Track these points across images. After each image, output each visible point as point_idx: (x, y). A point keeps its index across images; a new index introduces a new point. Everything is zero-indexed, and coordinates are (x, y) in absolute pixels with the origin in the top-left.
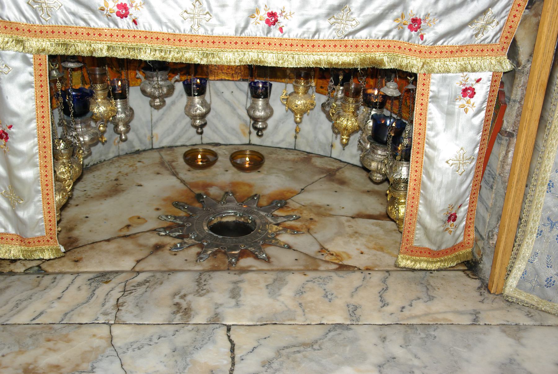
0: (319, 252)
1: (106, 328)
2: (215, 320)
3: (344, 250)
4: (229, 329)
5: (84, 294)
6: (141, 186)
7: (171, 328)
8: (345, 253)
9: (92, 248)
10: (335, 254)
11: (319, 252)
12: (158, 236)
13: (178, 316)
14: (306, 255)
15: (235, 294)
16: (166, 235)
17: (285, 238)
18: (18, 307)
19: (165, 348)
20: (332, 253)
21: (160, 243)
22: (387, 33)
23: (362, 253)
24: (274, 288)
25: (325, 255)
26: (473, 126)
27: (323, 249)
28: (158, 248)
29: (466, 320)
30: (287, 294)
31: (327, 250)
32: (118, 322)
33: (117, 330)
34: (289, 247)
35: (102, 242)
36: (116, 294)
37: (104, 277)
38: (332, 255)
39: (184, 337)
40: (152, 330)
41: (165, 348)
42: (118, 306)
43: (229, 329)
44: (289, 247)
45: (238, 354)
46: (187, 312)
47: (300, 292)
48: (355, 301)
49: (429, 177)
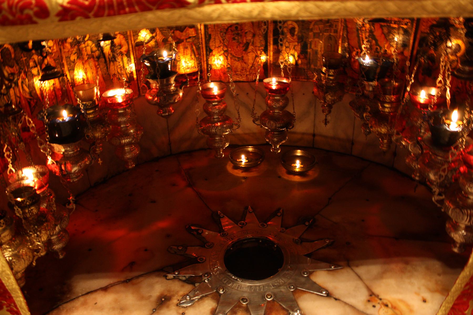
0: (369, 301)
3: (400, 296)
6: (154, 202)
8: (401, 301)
9: (84, 304)
10: (390, 305)
11: (369, 301)
12: (164, 280)
14: (352, 307)
16: (174, 278)
17: (322, 278)
20: (385, 302)
21: (166, 293)
23: (425, 301)
25: (378, 306)
27: (373, 296)
28: (163, 301)
31: (377, 296)
34: (329, 295)
35: (98, 292)
38: (387, 306)
44: (329, 295)
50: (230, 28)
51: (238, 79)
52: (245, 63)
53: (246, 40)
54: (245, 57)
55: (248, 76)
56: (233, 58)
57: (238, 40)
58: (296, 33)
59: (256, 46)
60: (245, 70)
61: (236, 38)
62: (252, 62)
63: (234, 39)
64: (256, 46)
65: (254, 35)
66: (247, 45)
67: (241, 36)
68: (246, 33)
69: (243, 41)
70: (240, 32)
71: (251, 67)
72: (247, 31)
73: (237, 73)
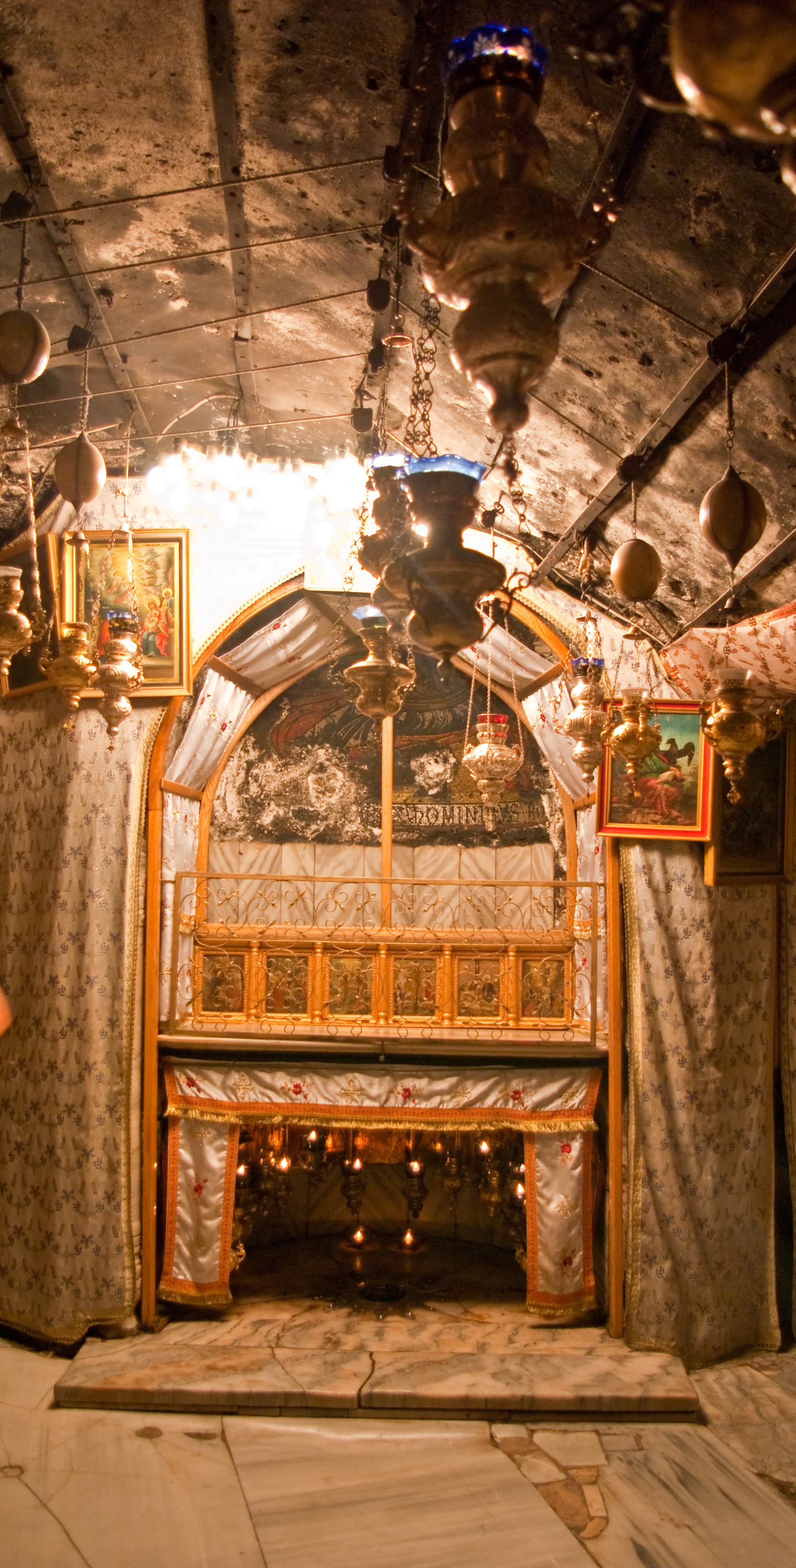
1: (269, 1351)
2: (361, 1348)
4: (371, 1354)
5: (249, 1330)
7: (322, 1352)
13: (329, 1346)
15: (380, 1334)
18: (195, 1336)
19: (318, 1361)
22: (496, 1102)
24: (412, 1333)
26: (572, 1177)
29: (582, 1353)
30: (425, 1336)
32: (278, 1346)
33: (278, 1351)
36: (276, 1331)
37: (263, 1322)
39: (334, 1356)
40: (305, 1353)
41: (318, 1361)
42: (278, 1338)
43: (371, 1354)
45: (377, 1366)
46: (337, 1343)
47: (438, 1334)
48: (487, 1340)
49: (542, 1222)
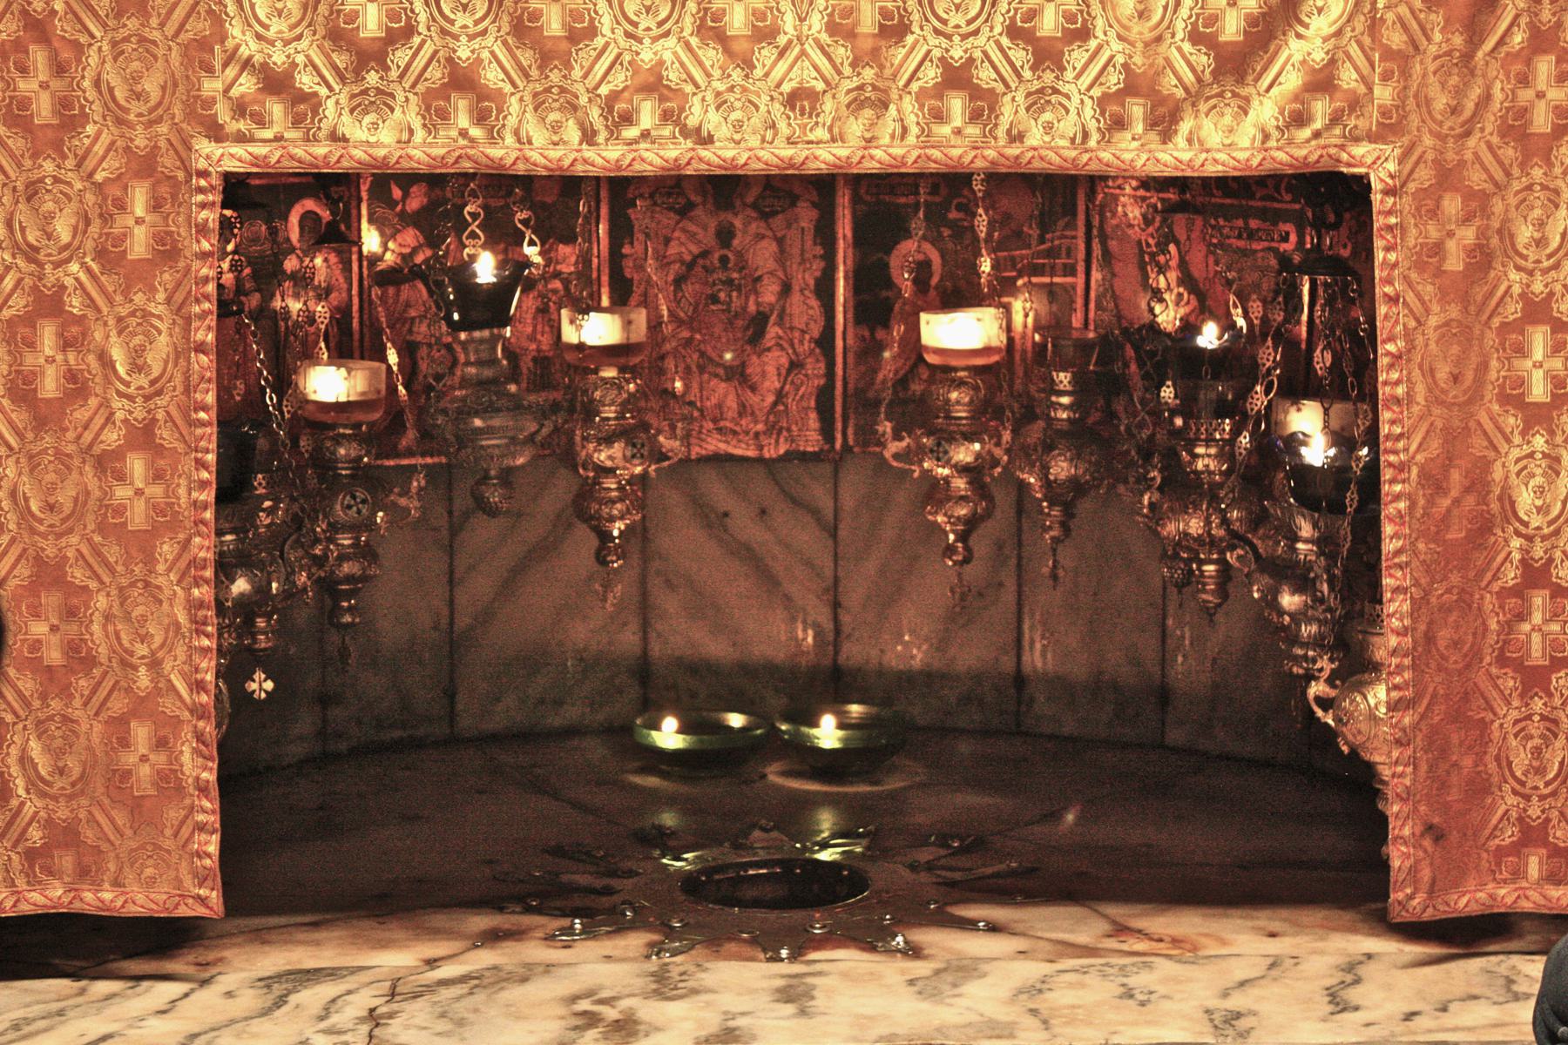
50: (701, 262)
51: (722, 446)
52: (753, 389)
53: (758, 304)
54: (753, 369)
55: (762, 437)
56: (711, 369)
57: (729, 304)
58: (935, 280)
59: (792, 329)
60: (753, 414)
61: (722, 295)
62: (777, 385)
63: (714, 299)
64: (792, 329)
65: (786, 289)
66: (759, 322)
67: (739, 289)
68: (759, 279)
69: (744, 308)
70: (735, 275)
71: (775, 404)
72: (759, 273)
73: (722, 424)
